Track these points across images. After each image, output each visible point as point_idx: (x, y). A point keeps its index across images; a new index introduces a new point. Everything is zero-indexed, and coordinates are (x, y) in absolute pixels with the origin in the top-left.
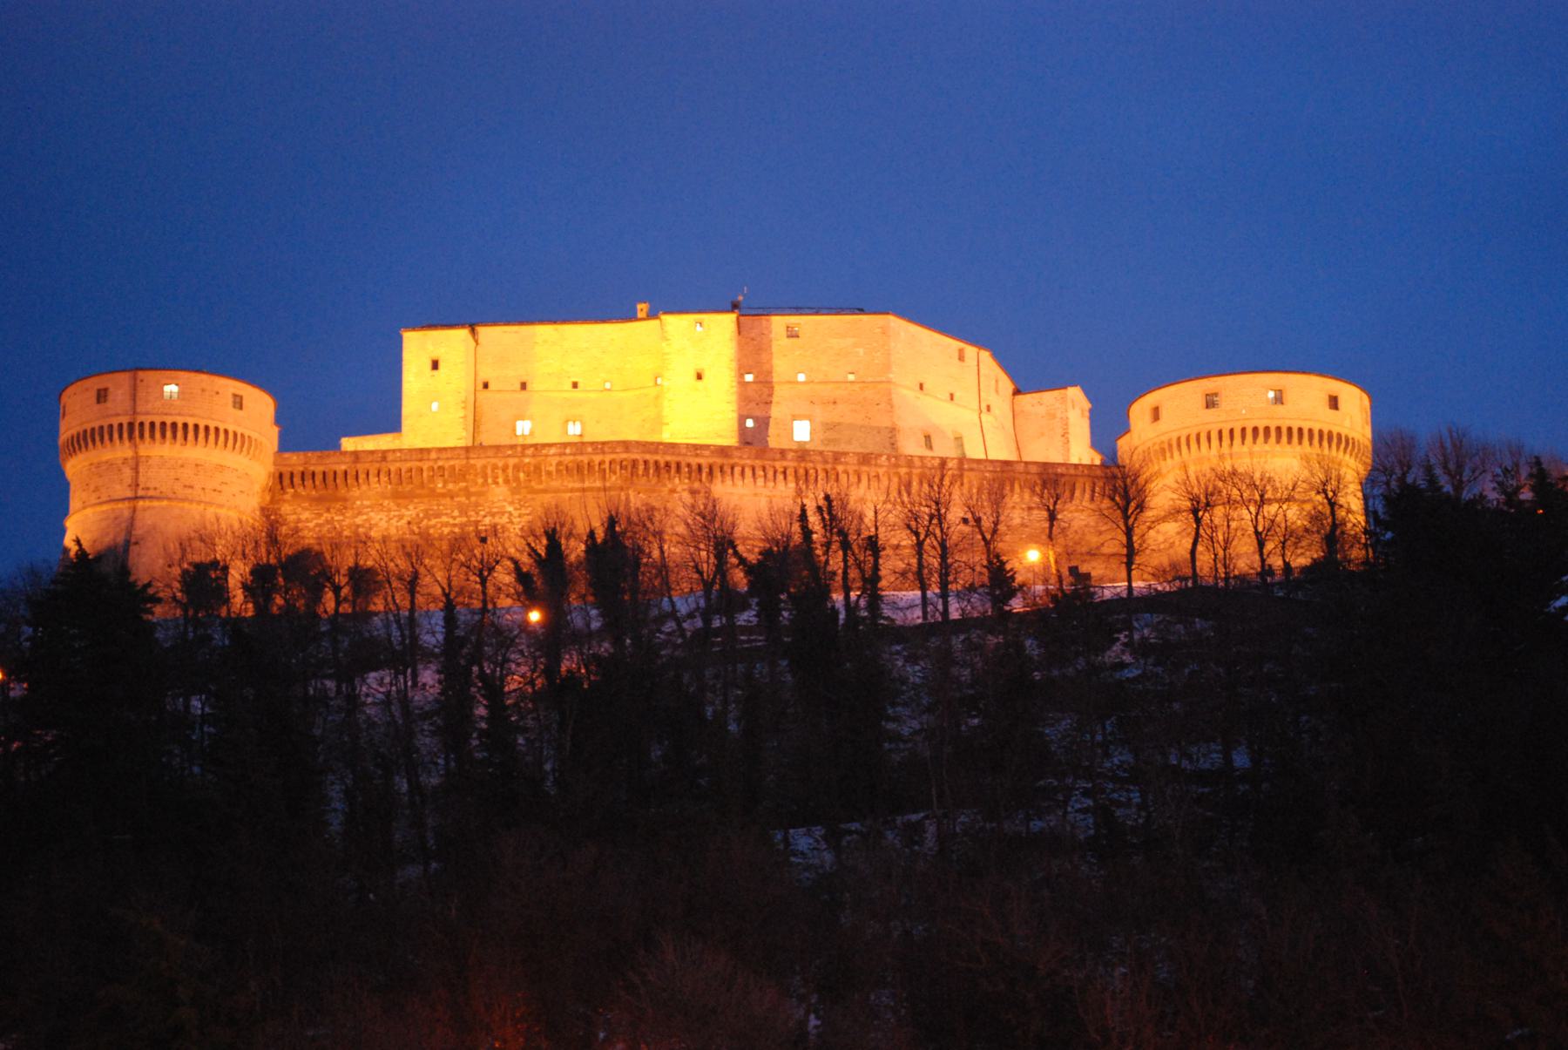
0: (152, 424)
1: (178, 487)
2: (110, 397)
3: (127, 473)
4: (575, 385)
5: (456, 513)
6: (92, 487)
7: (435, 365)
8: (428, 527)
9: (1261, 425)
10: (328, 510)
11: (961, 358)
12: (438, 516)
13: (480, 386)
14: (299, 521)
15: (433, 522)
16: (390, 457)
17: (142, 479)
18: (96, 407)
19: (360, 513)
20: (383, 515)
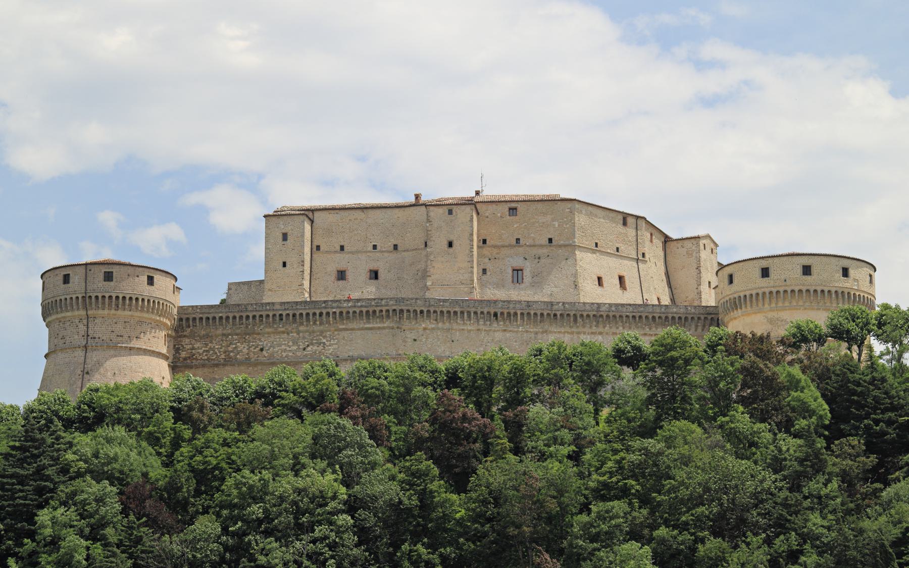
0: (97, 297)
1: (113, 336)
2: (71, 281)
3: (82, 328)
4: (375, 247)
5: (291, 344)
6: (60, 336)
7: (285, 237)
8: (273, 352)
9: (797, 289)
10: (211, 342)
11: (625, 224)
12: (280, 345)
13: (315, 249)
14: (193, 349)
15: (276, 349)
16: (250, 308)
17: (90, 332)
18: (63, 286)
19: (231, 344)
20: (245, 345)
